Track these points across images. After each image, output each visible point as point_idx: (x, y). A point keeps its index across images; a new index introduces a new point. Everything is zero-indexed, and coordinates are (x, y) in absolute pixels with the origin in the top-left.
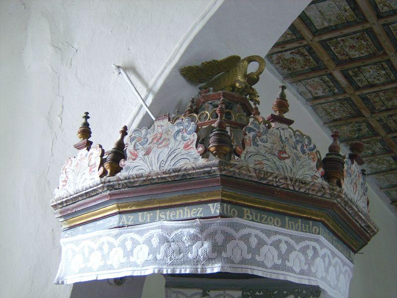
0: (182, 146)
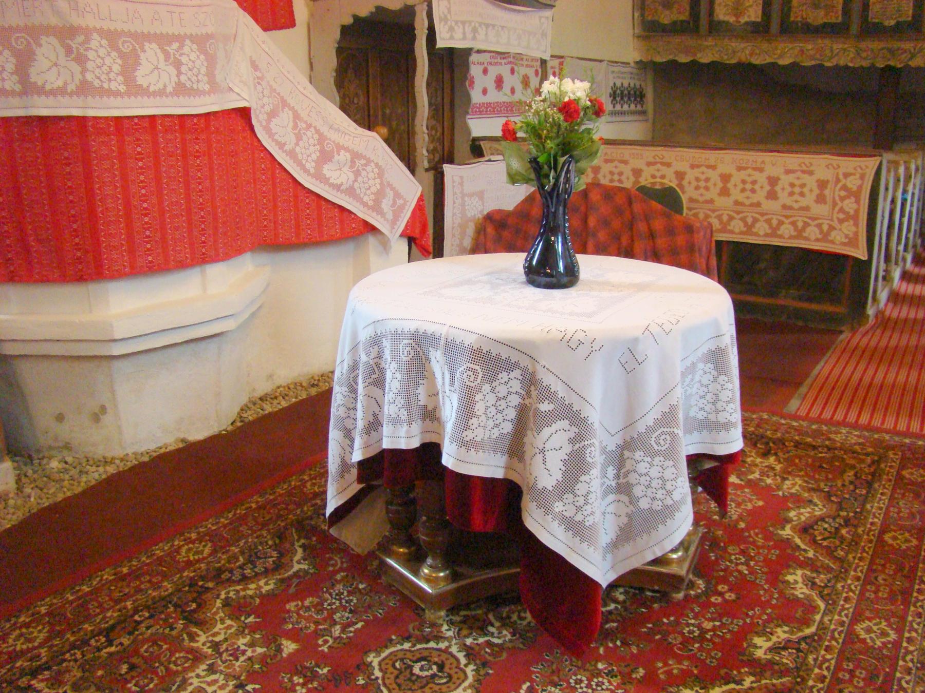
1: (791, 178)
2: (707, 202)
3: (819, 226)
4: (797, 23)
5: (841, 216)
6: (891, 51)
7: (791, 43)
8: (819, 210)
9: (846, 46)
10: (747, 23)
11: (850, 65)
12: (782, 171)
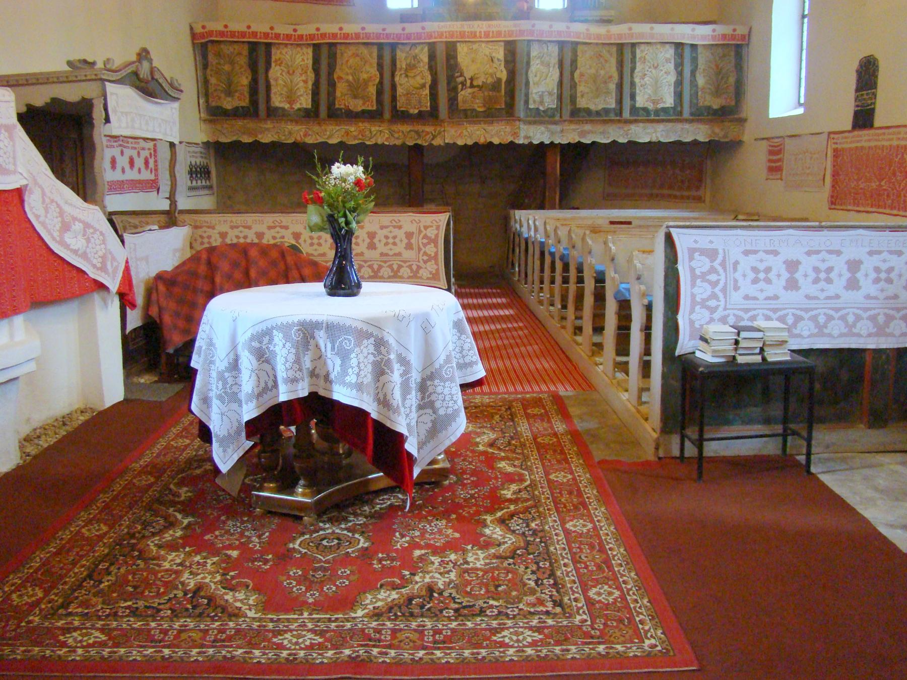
1: (385, 232)
3: (410, 267)
4: (341, 109)
5: (425, 258)
6: (417, 132)
7: (337, 125)
8: (407, 255)
9: (381, 129)
10: (299, 109)
11: (387, 143)
12: (378, 226)
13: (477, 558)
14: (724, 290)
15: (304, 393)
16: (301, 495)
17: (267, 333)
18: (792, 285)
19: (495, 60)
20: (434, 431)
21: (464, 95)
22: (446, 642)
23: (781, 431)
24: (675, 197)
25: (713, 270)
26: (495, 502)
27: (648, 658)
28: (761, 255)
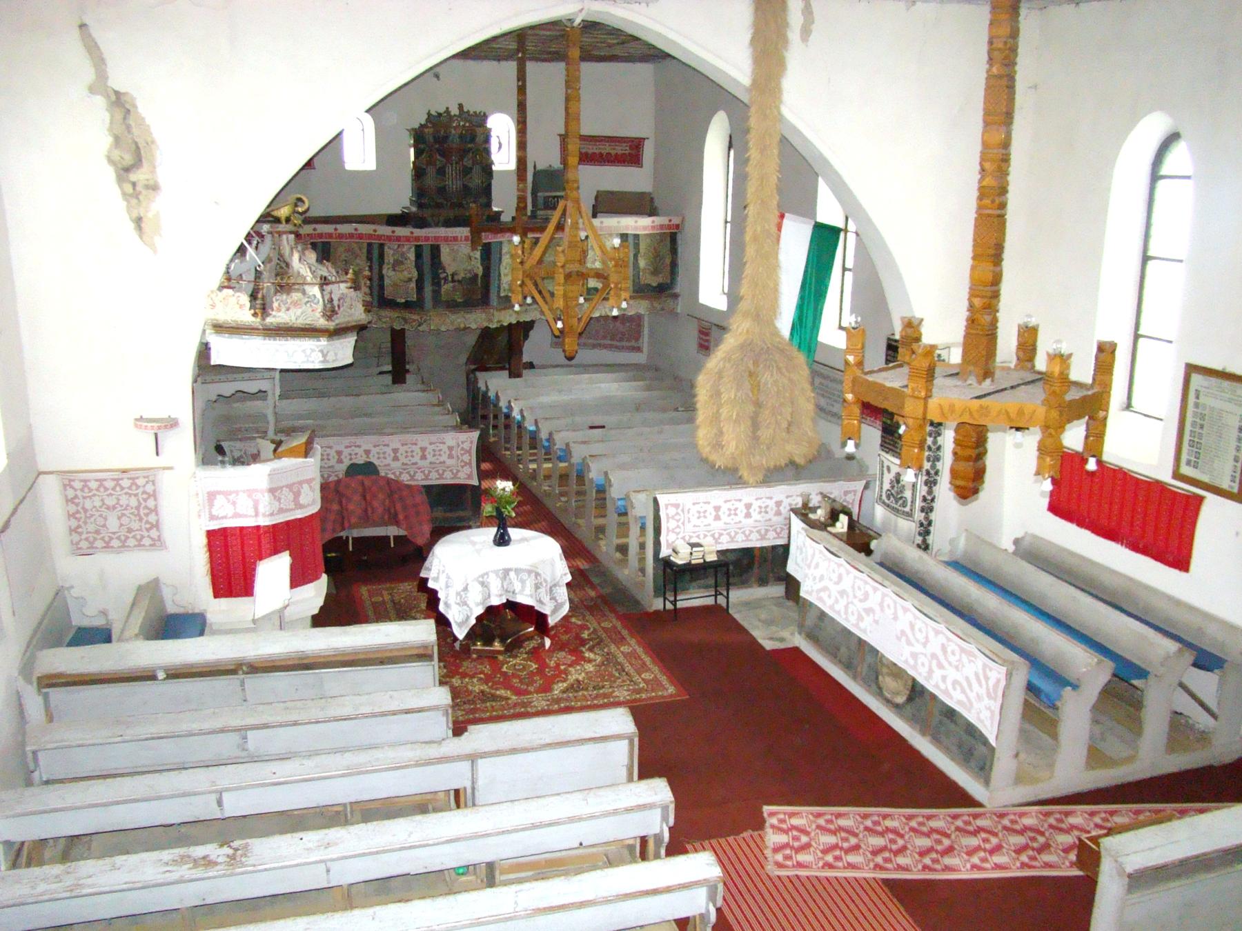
0: (310, 310)
1: (433, 447)
2: (385, 465)
13: (590, 667)
14: (683, 524)
15: (505, 601)
16: (497, 646)
17: (487, 574)
18: (717, 518)
19: (473, 259)
20: (554, 611)
21: (446, 288)
22: (597, 697)
23: (714, 593)
24: (617, 347)
25: (677, 514)
26: (583, 642)
27: (671, 696)
28: (702, 505)
